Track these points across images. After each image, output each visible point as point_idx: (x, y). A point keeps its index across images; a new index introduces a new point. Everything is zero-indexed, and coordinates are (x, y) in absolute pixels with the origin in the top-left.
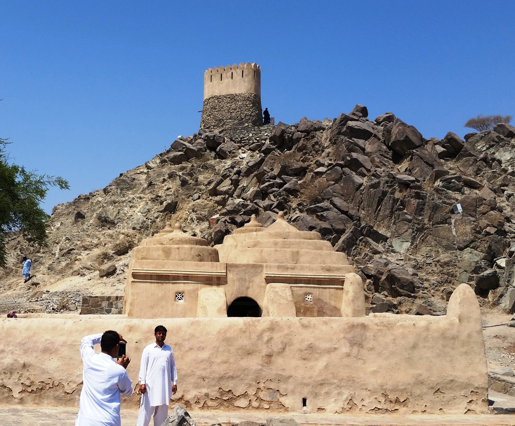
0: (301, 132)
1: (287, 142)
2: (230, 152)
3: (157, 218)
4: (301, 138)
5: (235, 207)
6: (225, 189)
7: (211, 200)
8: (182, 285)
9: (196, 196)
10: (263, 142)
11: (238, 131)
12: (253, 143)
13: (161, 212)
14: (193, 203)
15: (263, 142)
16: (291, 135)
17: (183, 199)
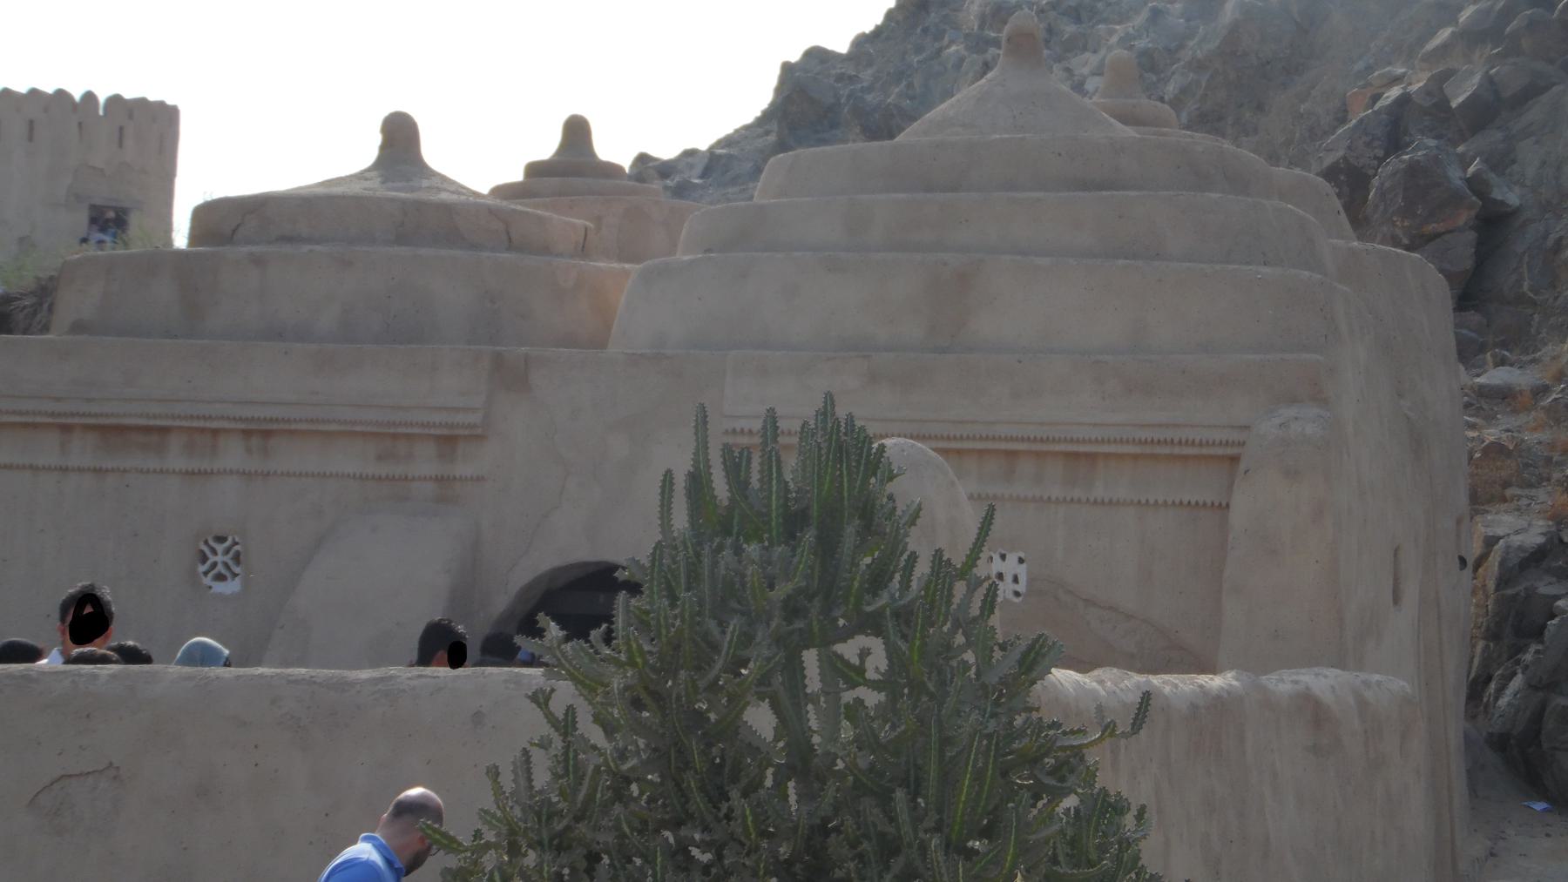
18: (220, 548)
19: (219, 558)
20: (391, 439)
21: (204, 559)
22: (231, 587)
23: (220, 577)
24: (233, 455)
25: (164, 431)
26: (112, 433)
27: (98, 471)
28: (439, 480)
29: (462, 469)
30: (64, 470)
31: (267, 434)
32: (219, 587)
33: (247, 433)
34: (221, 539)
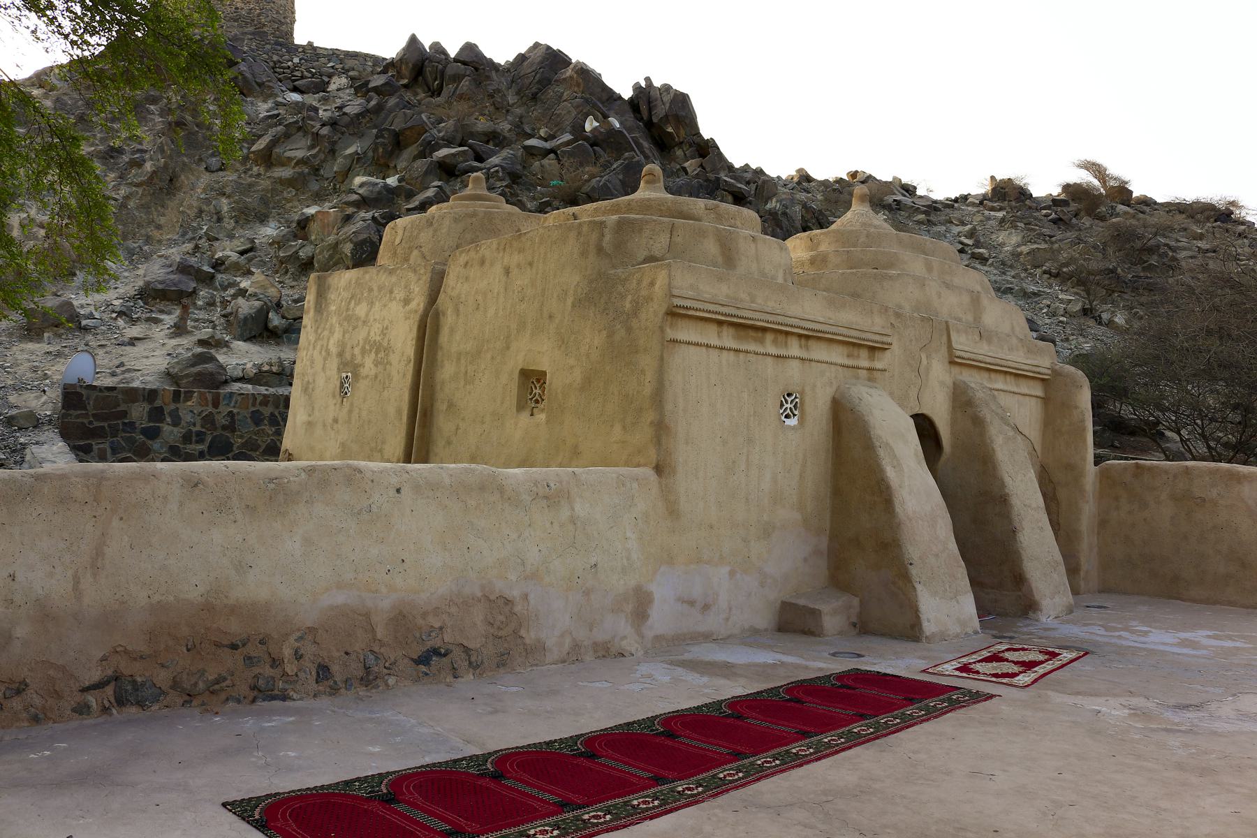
0: (464, 63)
1: (430, 79)
2: (260, 85)
3: (127, 198)
4: (464, 76)
5: (379, 193)
6: (300, 154)
7: (259, 175)
8: (795, 363)
9: (214, 162)
10: (326, 79)
11: (268, 47)
12: (302, 77)
13: (137, 185)
14: (215, 176)
15: (326, 79)
16: (440, 67)
17: (184, 164)
18: (789, 400)
19: (789, 406)
20: (853, 345)
21: (782, 405)
22: (792, 422)
23: (787, 417)
24: (794, 349)
25: (764, 330)
26: (743, 328)
27: (736, 351)
28: (869, 369)
29: (879, 365)
30: (722, 348)
31: (808, 337)
32: (788, 422)
33: (800, 336)
34: (789, 395)
